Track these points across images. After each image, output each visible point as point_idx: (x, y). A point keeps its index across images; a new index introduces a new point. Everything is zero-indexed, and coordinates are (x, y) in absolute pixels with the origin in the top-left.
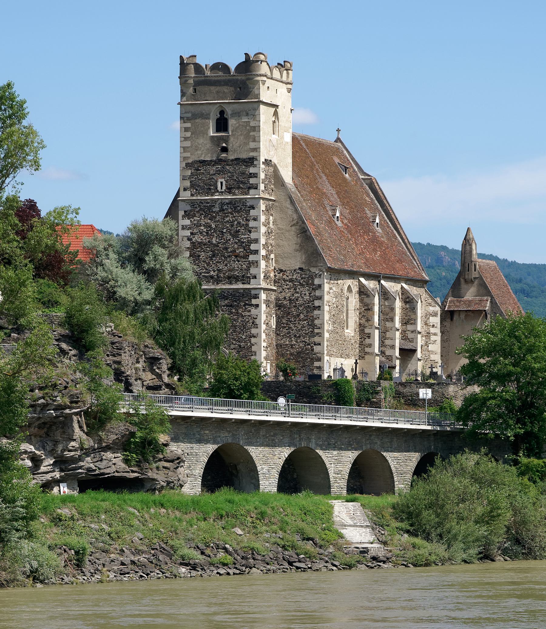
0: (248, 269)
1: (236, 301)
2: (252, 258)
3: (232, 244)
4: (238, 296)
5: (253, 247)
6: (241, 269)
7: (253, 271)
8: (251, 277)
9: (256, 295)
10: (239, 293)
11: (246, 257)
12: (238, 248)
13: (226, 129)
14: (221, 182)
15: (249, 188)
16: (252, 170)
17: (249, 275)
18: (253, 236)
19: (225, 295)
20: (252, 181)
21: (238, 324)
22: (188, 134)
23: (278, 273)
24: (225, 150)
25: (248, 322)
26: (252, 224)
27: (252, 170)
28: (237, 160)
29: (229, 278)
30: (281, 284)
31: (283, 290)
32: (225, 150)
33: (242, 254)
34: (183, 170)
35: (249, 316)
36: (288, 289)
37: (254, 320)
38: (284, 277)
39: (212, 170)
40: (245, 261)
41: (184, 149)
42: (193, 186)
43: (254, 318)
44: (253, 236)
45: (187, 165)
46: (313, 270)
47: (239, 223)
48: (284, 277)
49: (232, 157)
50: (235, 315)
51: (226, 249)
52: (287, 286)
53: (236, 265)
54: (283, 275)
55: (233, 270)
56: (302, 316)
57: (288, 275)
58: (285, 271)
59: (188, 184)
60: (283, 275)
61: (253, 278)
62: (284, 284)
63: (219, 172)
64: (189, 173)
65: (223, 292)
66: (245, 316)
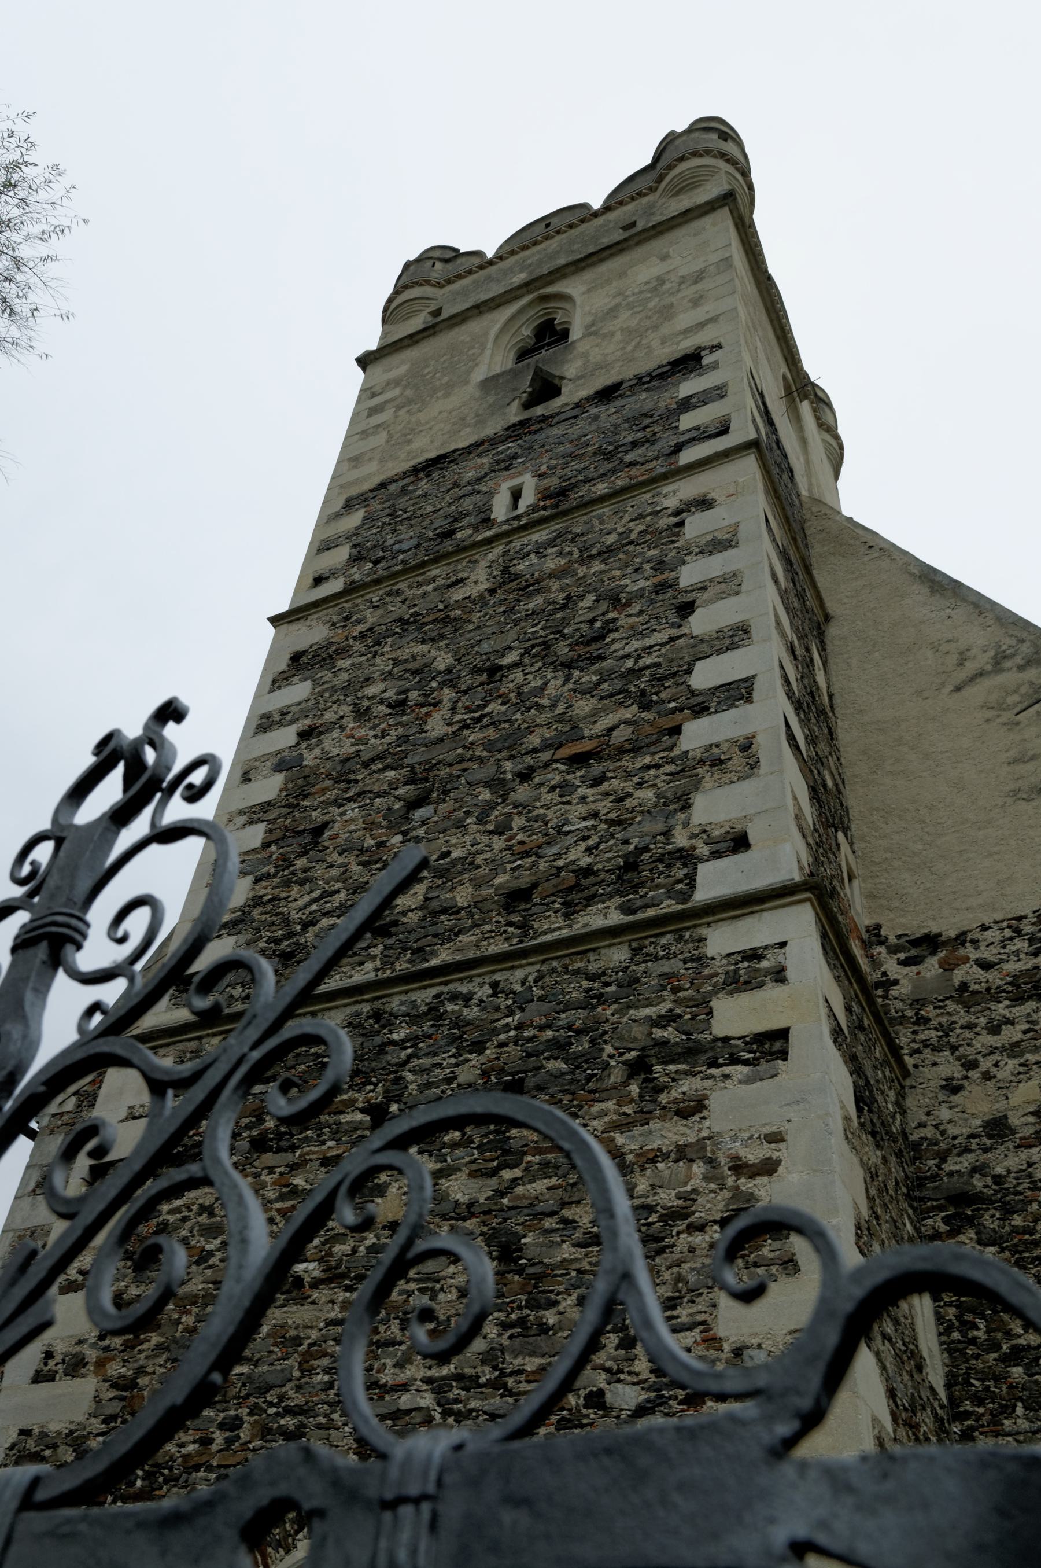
1: (559, 1047)
4: (585, 1005)
6: (611, 823)
8: (703, 850)
9: (754, 955)
10: (592, 977)
12: (593, 716)
17: (681, 840)
19: (472, 1013)
21: (567, 1251)
23: (905, 963)
25: (681, 1214)
30: (946, 1031)
31: (971, 1065)
33: (621, 735)
35: (682, 1153)
36: (1014, 1049)
37: (746, 1184)
38: (958, 976)
40: (648, 767)
43: (739, 1167)
48: (958, 976)
50: (546, 1169)
52: (994, 1029)
54: (948, 966)
57: (987, 954)
58: (961, 939)
60: (948, 966)
61: (716, 855)
62: (969, 1026)
65: (454, 997)
66: (655, 1157)
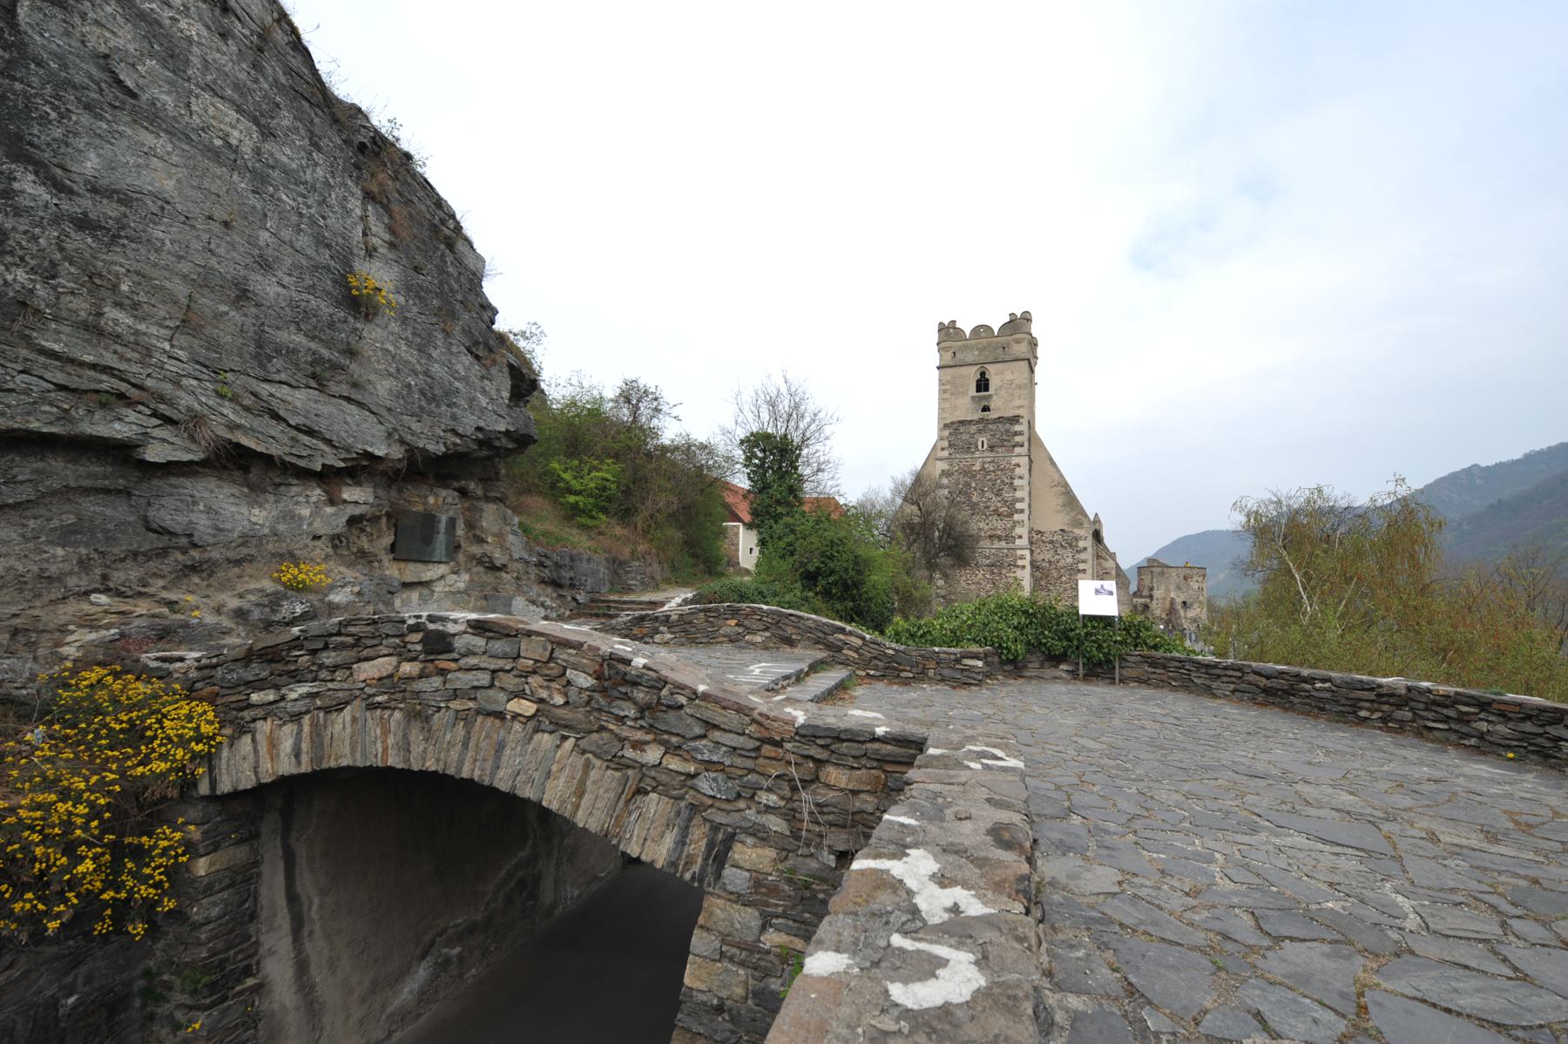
0: (1013, 527)
2: (1017, 517)
3: (995, 502)
5: (1018, 506)
7: (1018, 531)
11: (1010, 515)
13: (987, 389)
14: (983, 440)
15: (1014, 446)
16: (1017, 428)
18: (1018, 494)
20: (1017, 439)
22: (947, 396)
24: (986, 409)
26: (1017, 482)
27: (1017, 428)
28: (1000, 420)
29: (991, 537)
32: (986, 409)
34: (941, 430)
39: (973, 428)
41: (942, 410)
42: (950, 446)
44: (1018, 494)
45: (946, 426)
46: (1077, 531)
47: (1003, 481)
49: (996, 416)
51: (987, 507)
53: (999, 524)
55: (996, 528)
56: (1064, 579)
59: (945, 444)
63: (980, 431)
64: (946, 433)
